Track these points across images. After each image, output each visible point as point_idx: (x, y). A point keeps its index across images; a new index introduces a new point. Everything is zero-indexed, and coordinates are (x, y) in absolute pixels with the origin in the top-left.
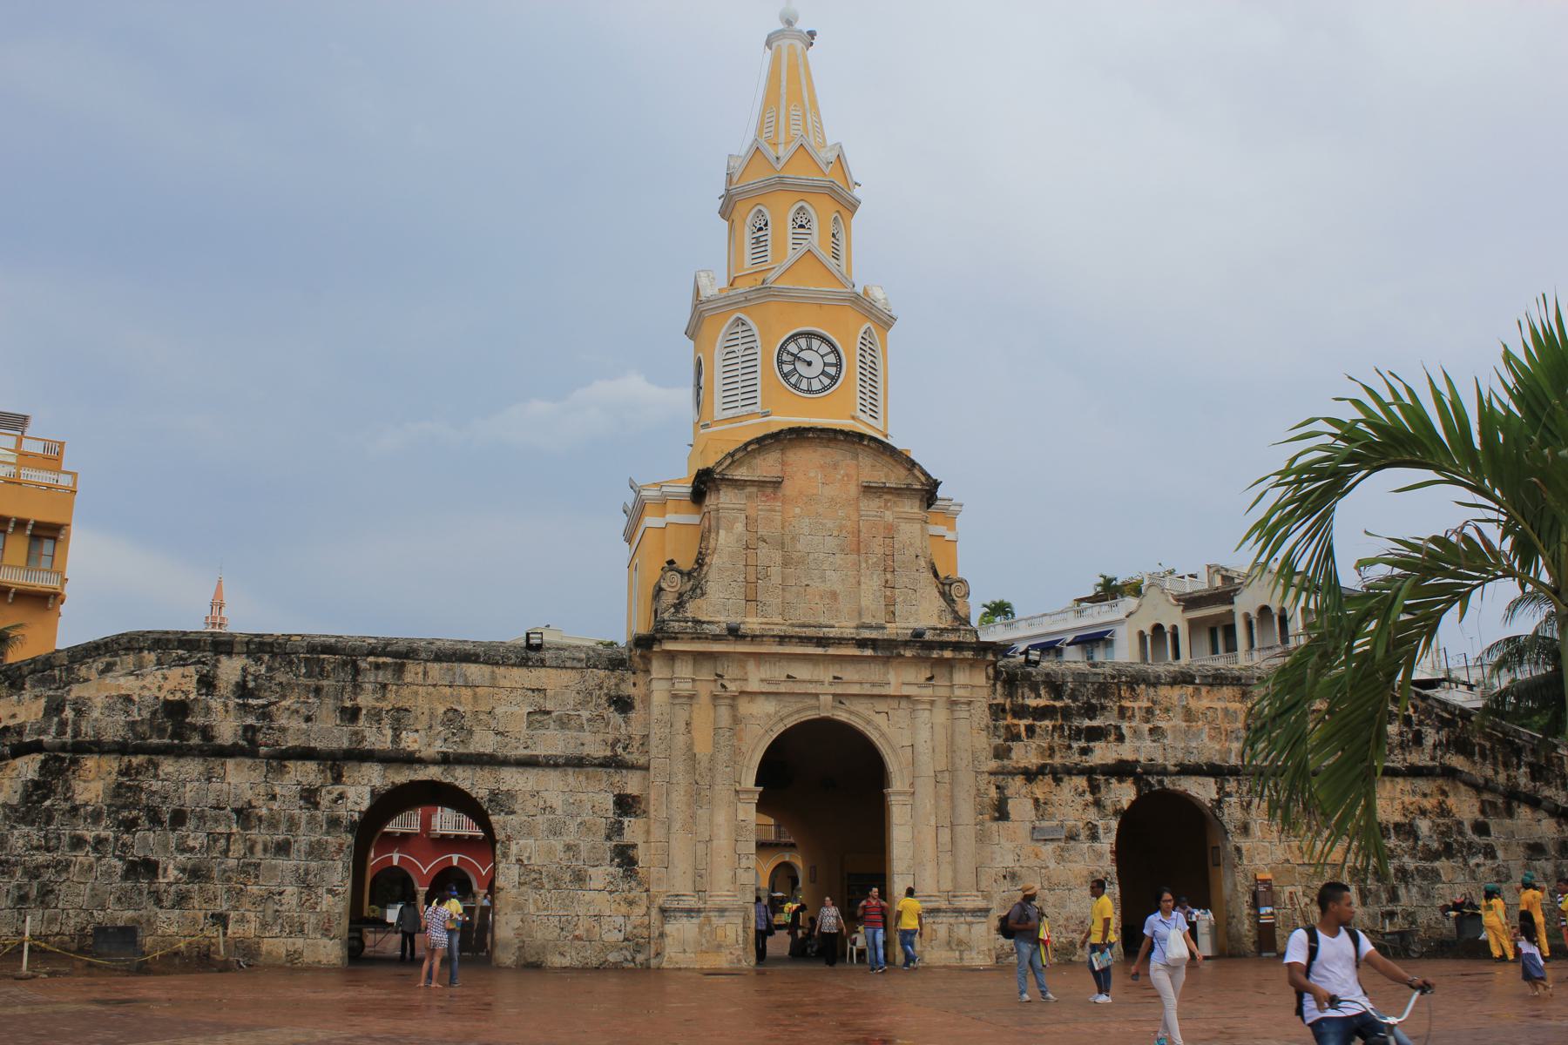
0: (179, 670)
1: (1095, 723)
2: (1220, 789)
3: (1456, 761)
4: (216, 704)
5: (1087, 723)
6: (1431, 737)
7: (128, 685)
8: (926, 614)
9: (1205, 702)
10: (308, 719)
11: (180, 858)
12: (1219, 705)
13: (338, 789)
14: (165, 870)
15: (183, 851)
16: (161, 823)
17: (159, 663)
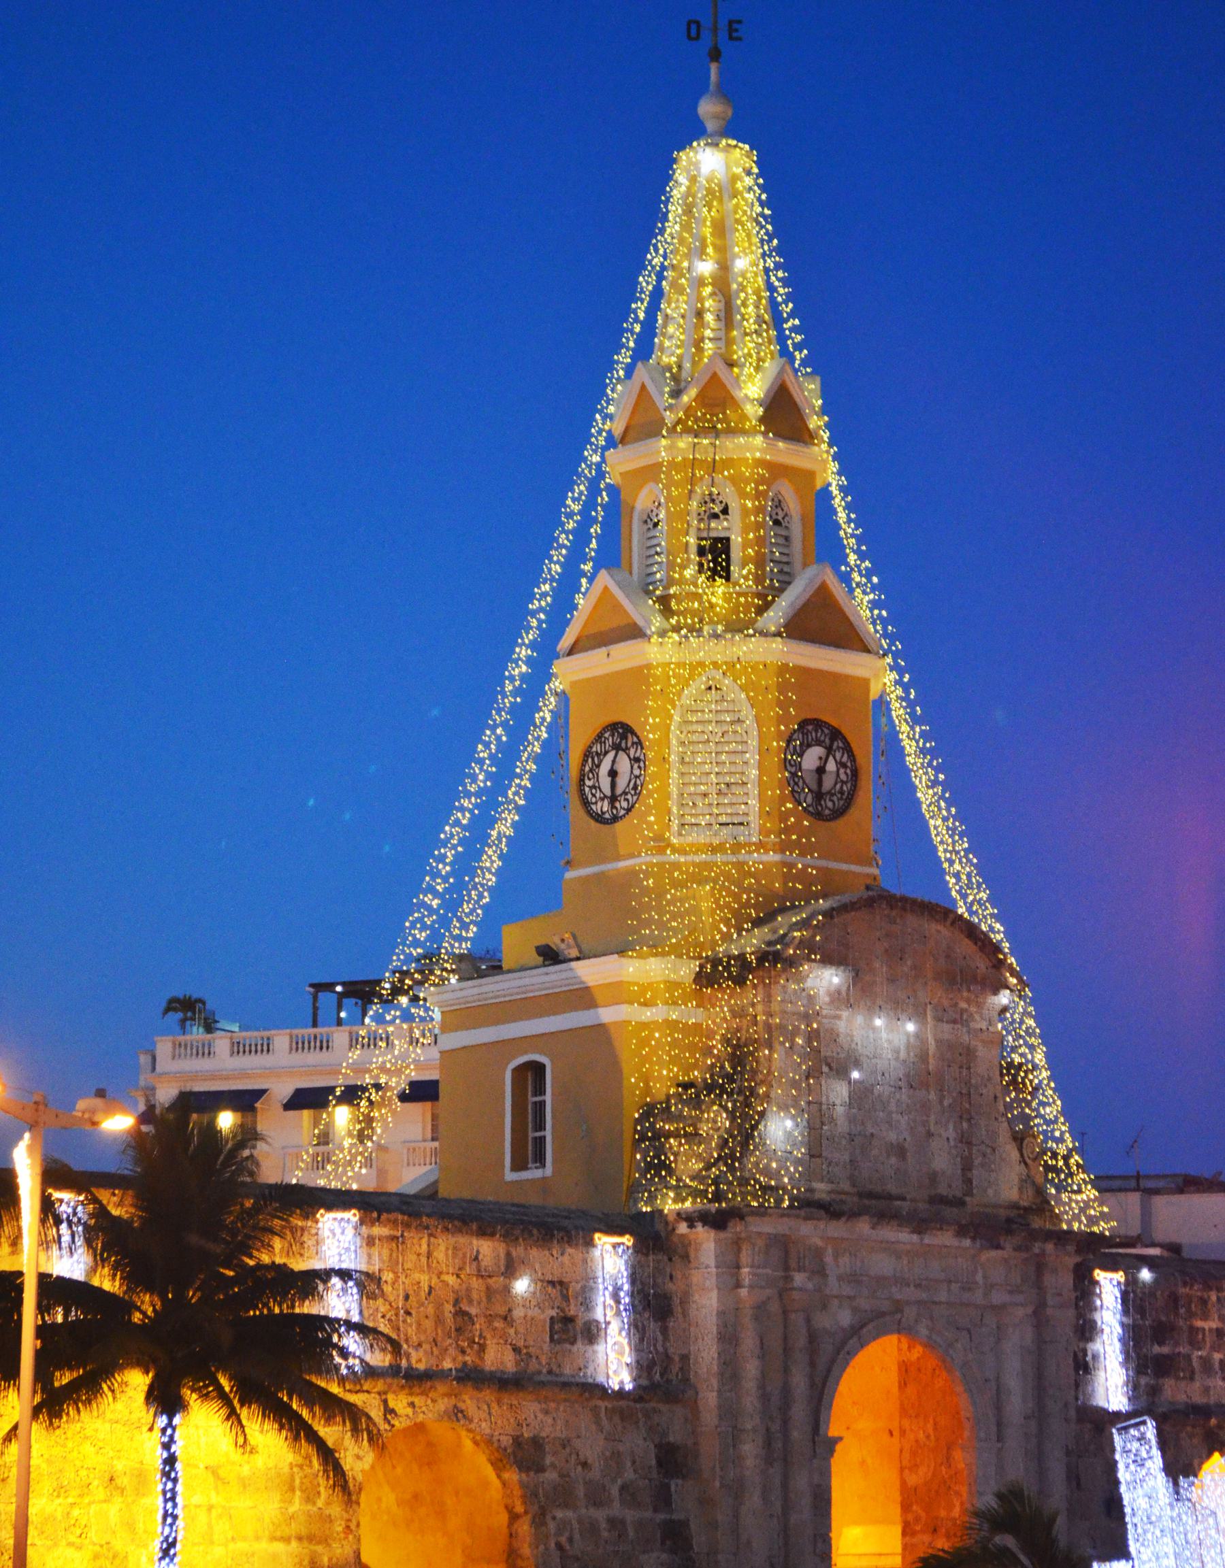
1: (1165, 1350)
5: (1157, 1349)
8: (1006, 1185)
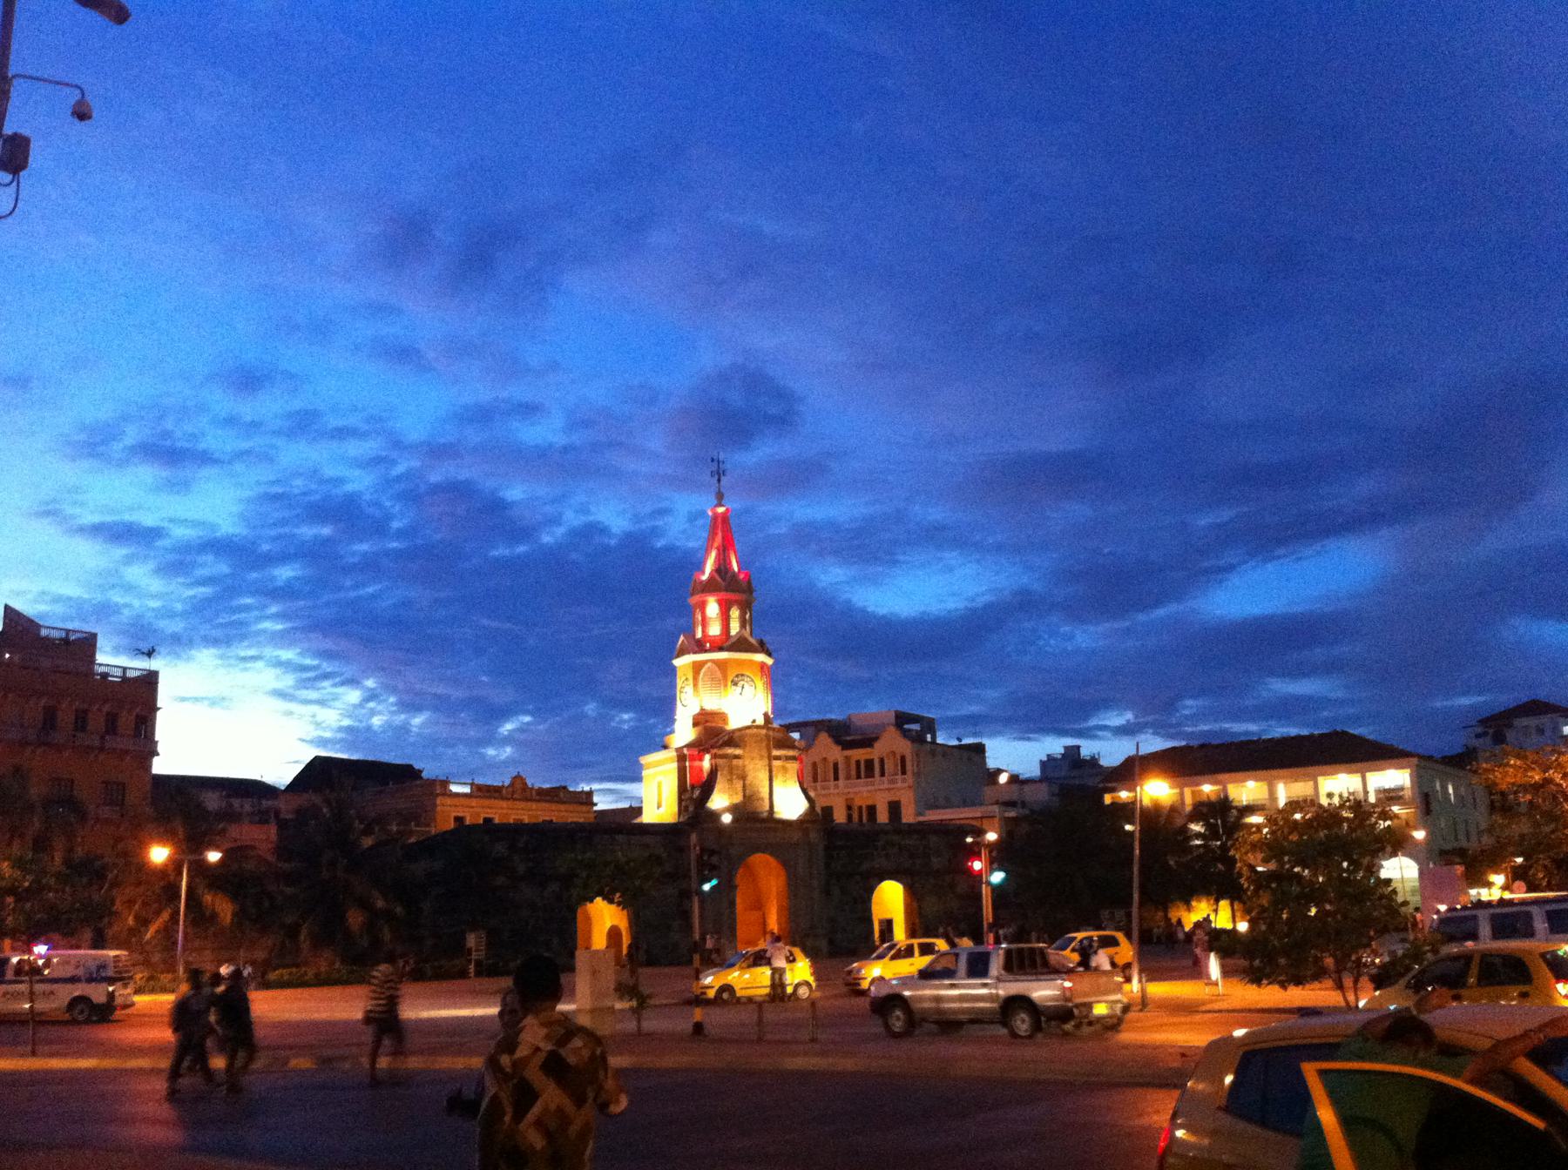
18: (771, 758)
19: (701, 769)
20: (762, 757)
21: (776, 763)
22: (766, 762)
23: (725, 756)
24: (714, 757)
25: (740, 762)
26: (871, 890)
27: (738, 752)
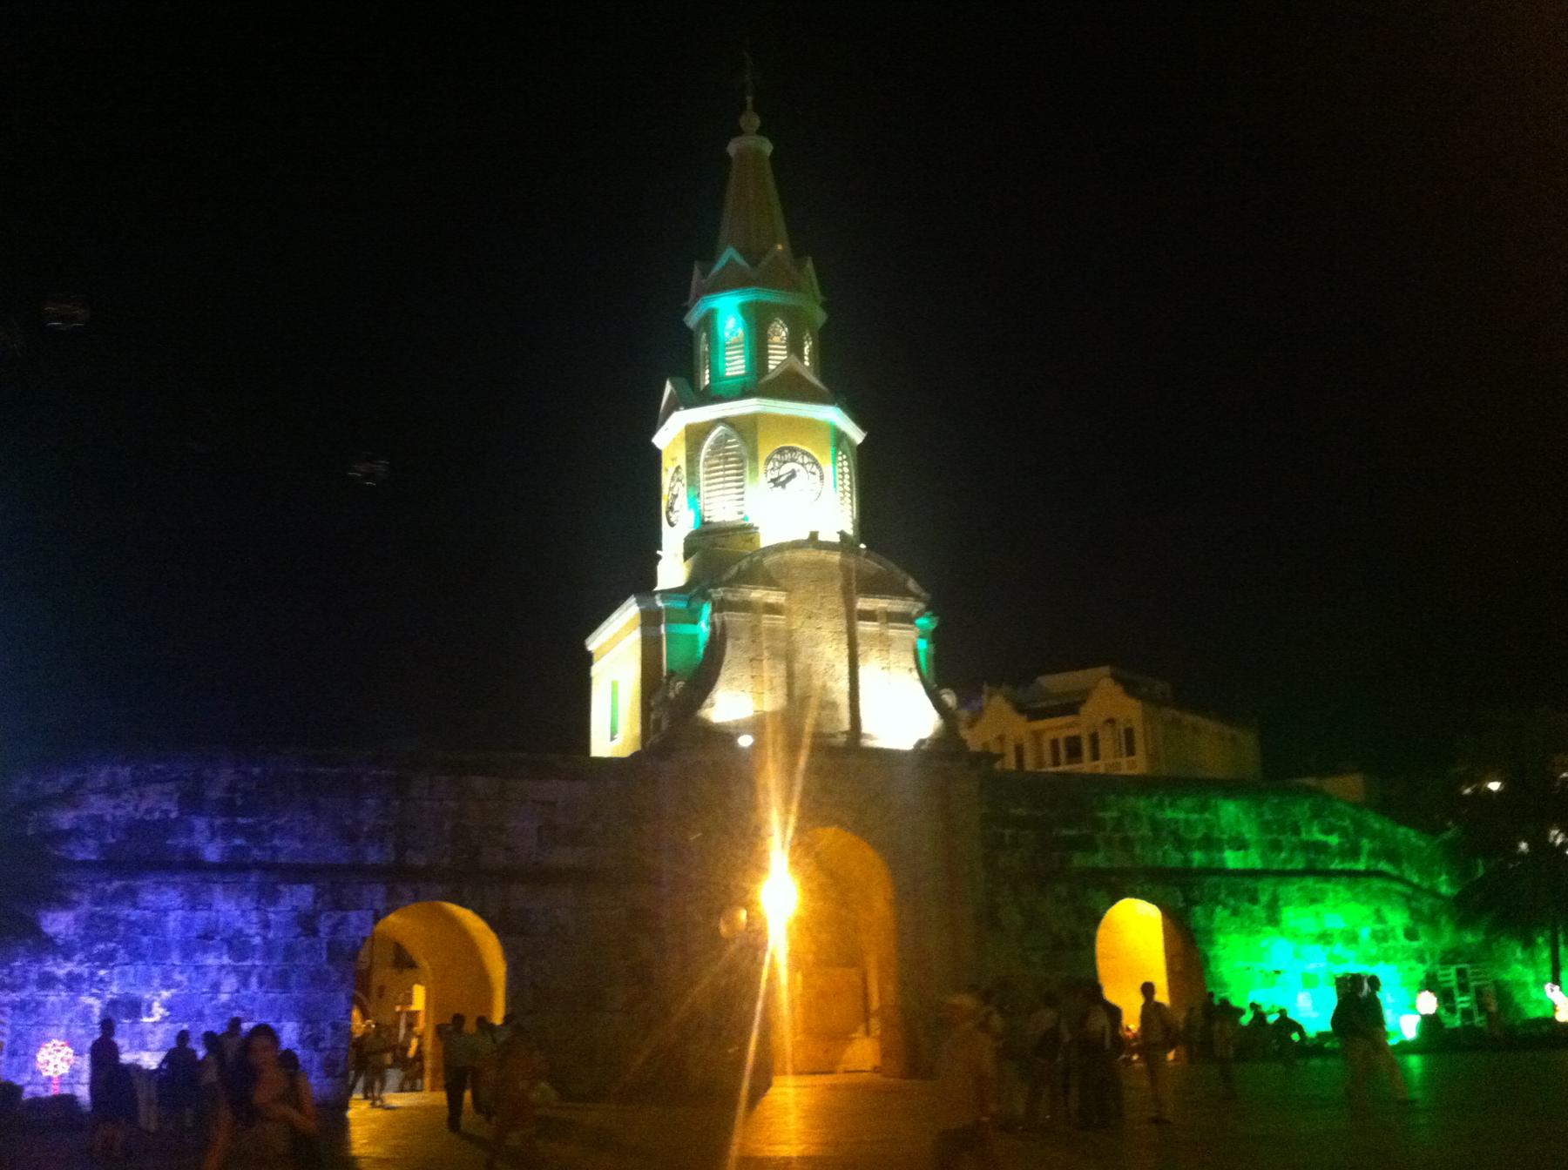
0: (158, 787)
1: (1073, 832)
2: (1186, 899)
3: (1384, 866)
4: (201, 824)
5: (1065, 832)
6: (1366, 844)
7: (98, 805)
9: (1169, 814)
10: (303, 839)
11: (166, 994)
12: (1181, 816)
13: (338, 915)
14: (150, 1008)
15: (168, 988)
16: (142, 957)
17: (136, 782)
18: (853, 617)
19: (694, 638)
20: (833, 615)
21: (865, 627)
22: (841, 624)
23: (746, 606)
24: (719, 606)
25: (780, 621)
26: (1096, 919)
27: (774, 597)
